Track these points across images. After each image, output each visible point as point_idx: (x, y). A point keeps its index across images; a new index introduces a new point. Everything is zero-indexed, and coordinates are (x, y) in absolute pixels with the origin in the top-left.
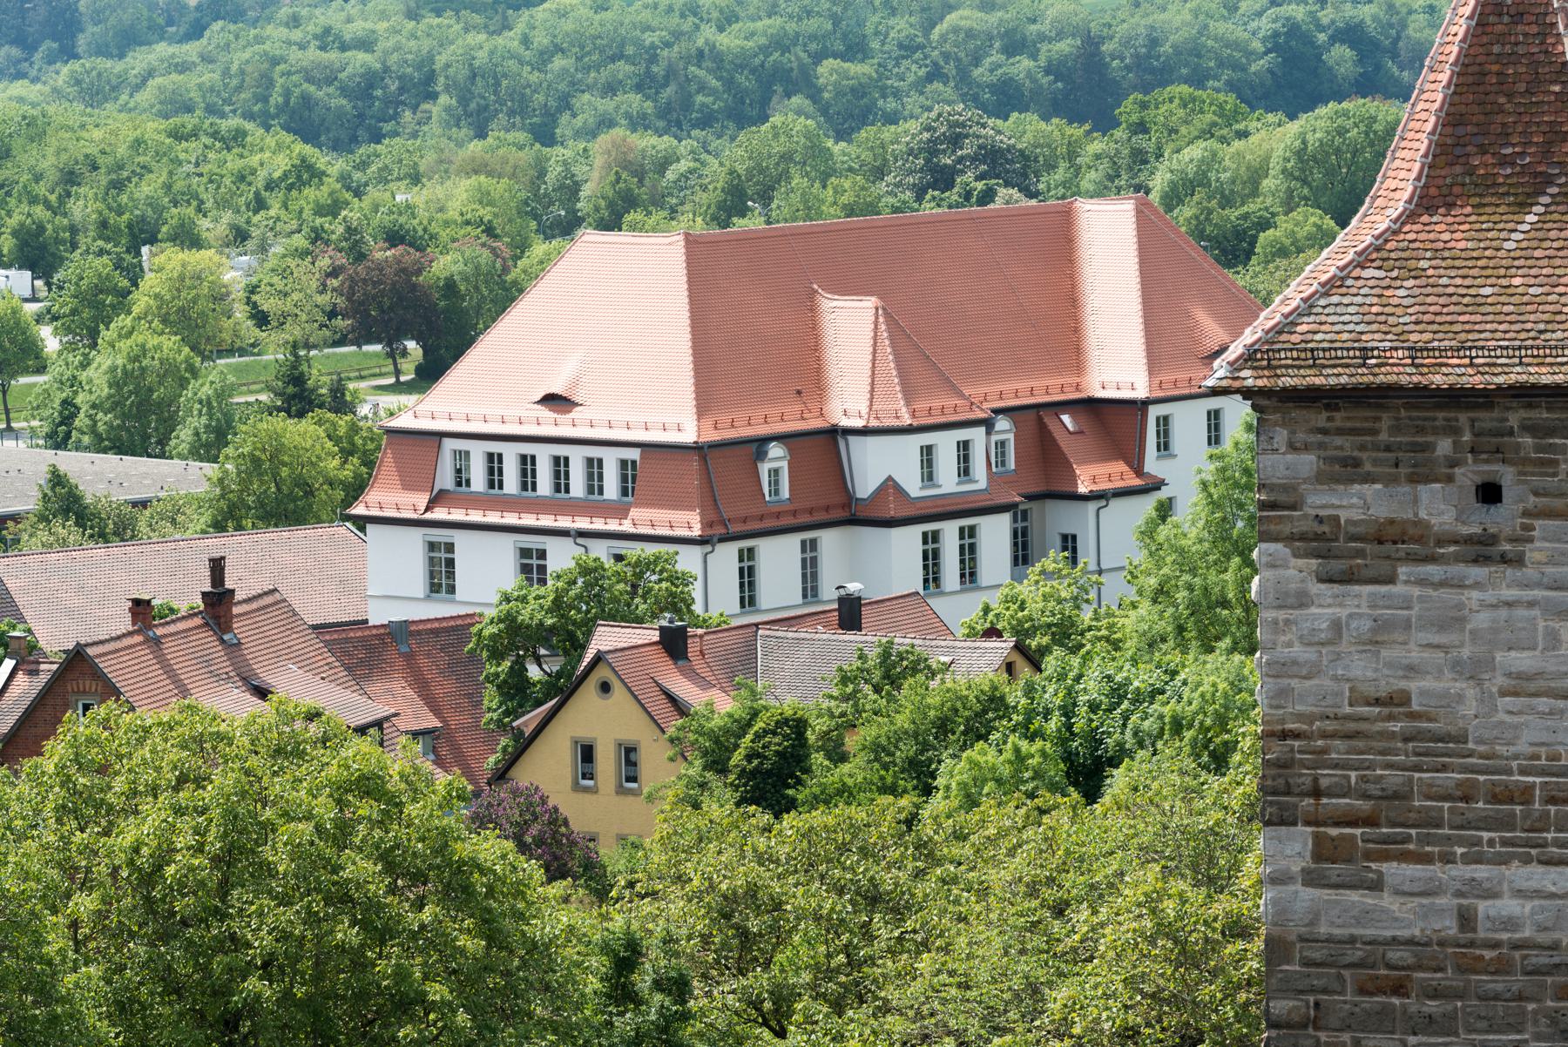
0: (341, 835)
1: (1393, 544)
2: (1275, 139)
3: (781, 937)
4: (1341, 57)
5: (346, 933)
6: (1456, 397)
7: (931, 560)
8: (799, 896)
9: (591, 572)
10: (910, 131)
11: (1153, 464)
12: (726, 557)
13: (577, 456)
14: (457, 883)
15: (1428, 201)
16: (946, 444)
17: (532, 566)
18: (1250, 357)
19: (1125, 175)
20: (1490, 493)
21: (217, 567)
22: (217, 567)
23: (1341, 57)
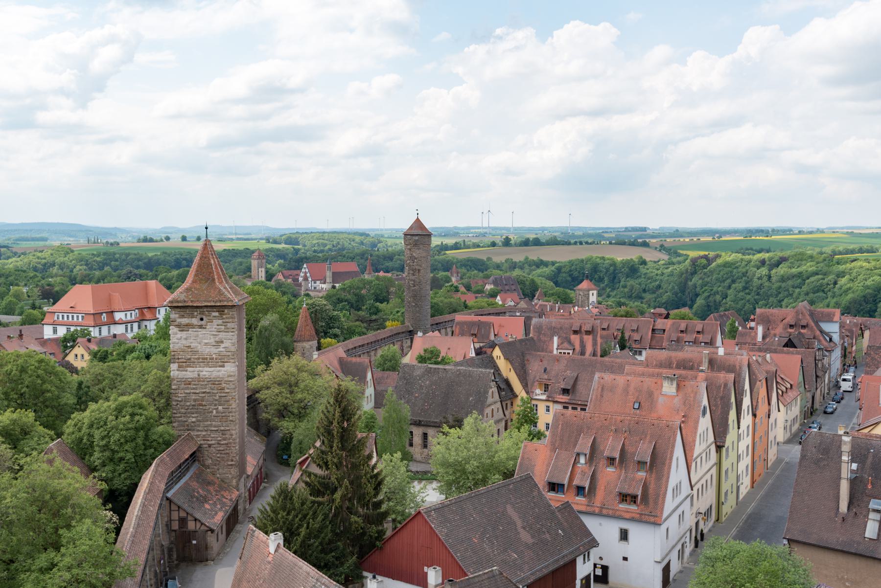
0: (38, 368)
1: (189, 326)
2: (175, 273)
3: (104, 380)
4: (184, 263)
5: (39, 381)
6: (197, 307)
7: (126, 329)
8: (106, 374)
9: (76, 330)
10: (124, 271)
11: (158, 316)
12: (97, 329)
13: (75, 315)
14: (56, 374)
15: (194, 282)
16: (129, 313)
17: (68, 330)
18: (170, 302)
19: (155, 277)
20: (202, 319)
21: (21, 331)
22: (21, 331)
23: (184, 263)
